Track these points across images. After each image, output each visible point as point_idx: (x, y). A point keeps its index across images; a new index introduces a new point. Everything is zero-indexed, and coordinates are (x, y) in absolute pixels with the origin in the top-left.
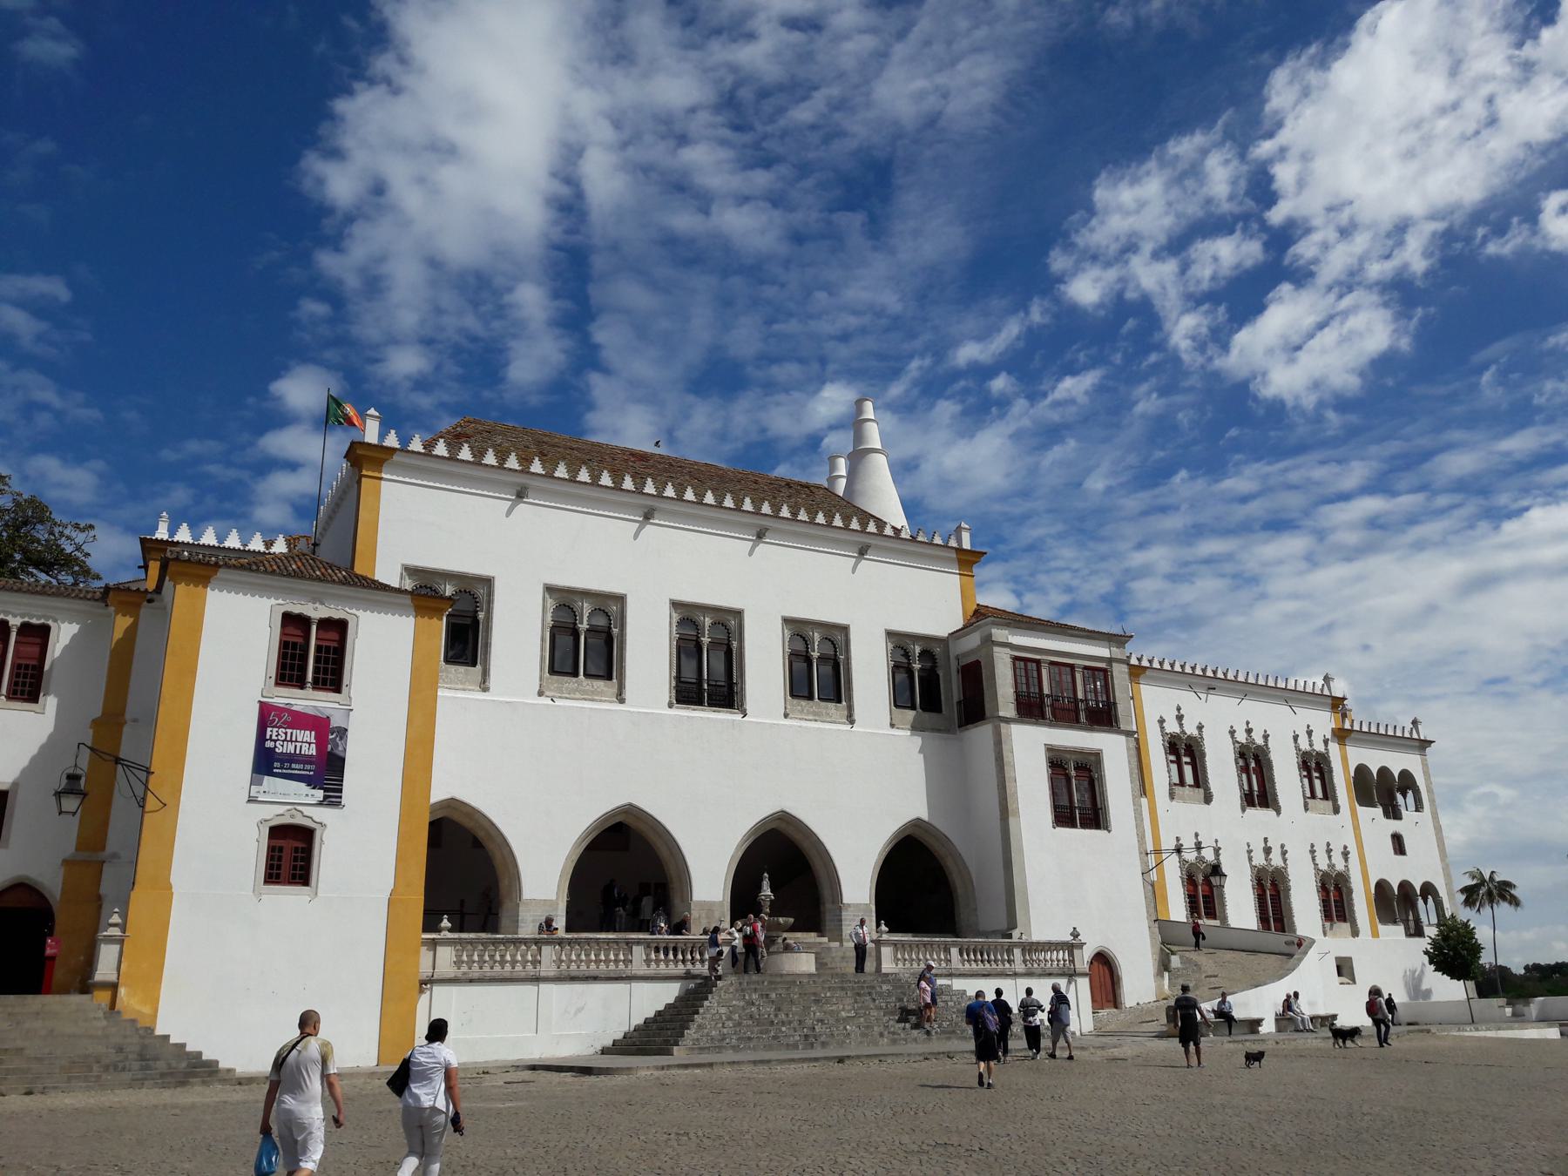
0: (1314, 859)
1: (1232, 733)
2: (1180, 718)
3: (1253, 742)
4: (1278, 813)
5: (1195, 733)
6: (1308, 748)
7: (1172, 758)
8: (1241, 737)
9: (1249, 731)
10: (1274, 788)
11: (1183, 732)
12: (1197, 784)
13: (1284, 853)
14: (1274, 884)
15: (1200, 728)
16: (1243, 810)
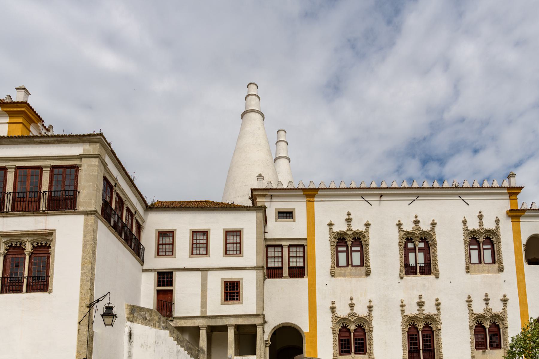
0: (469, 306)
1: (399, 225)
2: (349, 221)
3: (419, 229)
4: (437, 278)
5: (362, 229)
6: (477, 227)
7: (344, 249)
8: (408, 227)
9: (416, 222)
10: (435, 259)
11: (350, 230)
12: (362, 264)
13: (438, 305)
14: (427, 327)
15: (368, 225)
16: (402, 278)
